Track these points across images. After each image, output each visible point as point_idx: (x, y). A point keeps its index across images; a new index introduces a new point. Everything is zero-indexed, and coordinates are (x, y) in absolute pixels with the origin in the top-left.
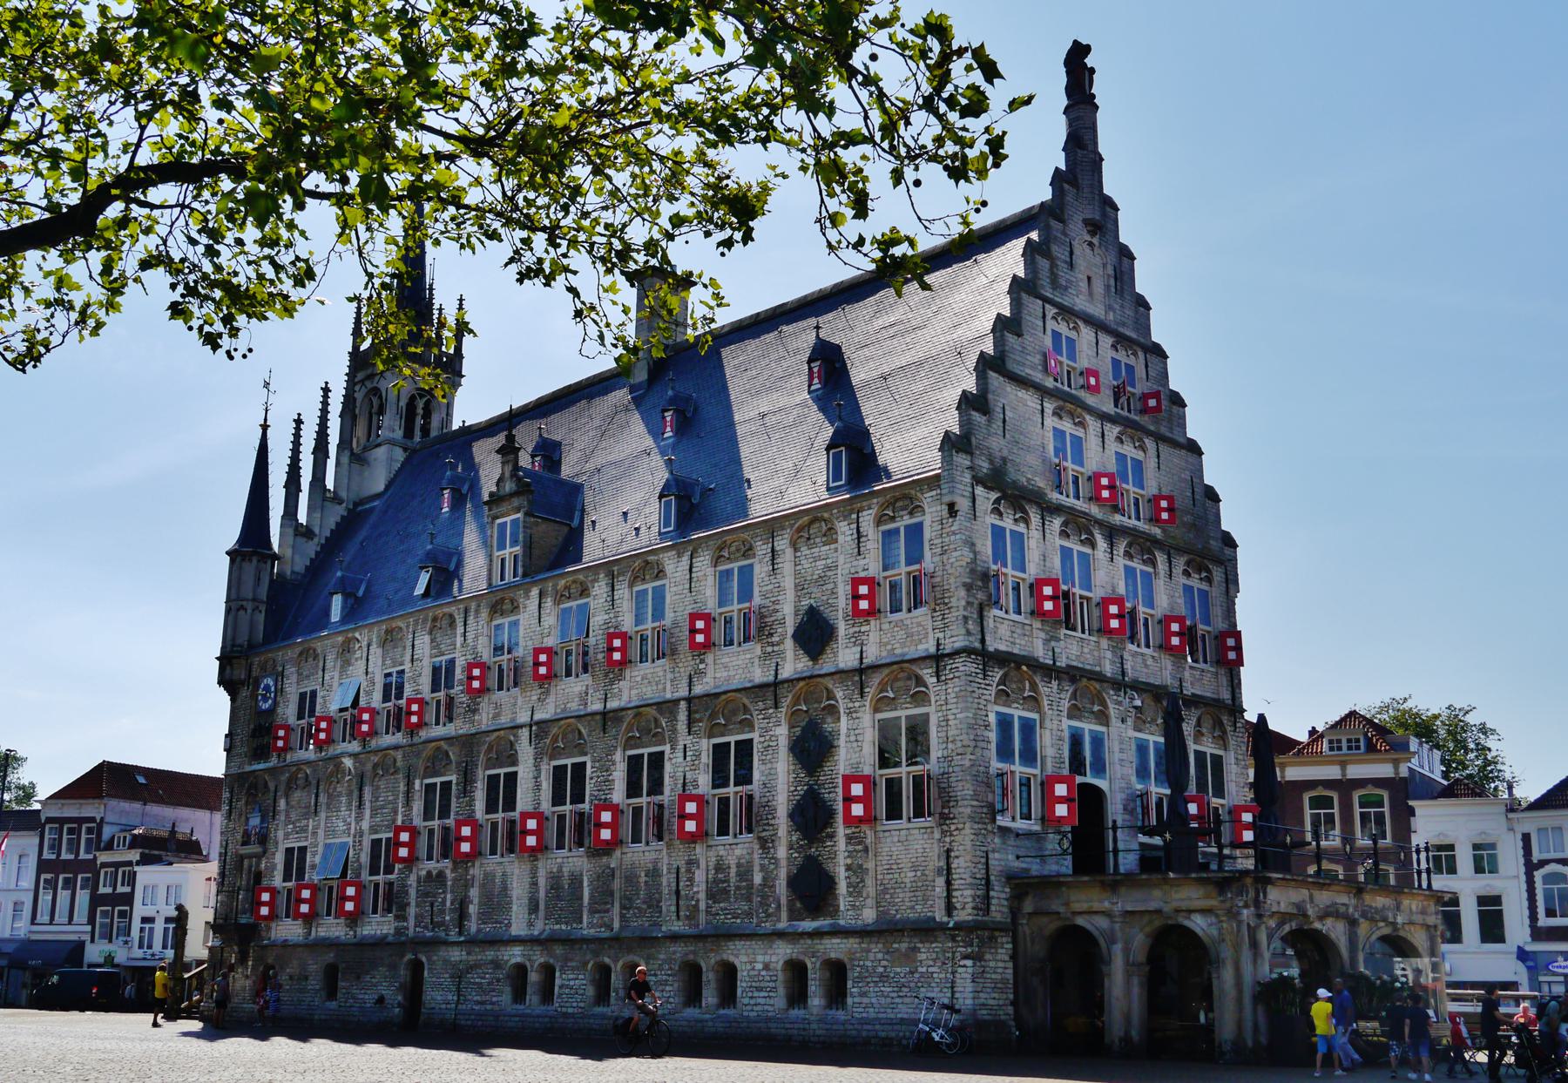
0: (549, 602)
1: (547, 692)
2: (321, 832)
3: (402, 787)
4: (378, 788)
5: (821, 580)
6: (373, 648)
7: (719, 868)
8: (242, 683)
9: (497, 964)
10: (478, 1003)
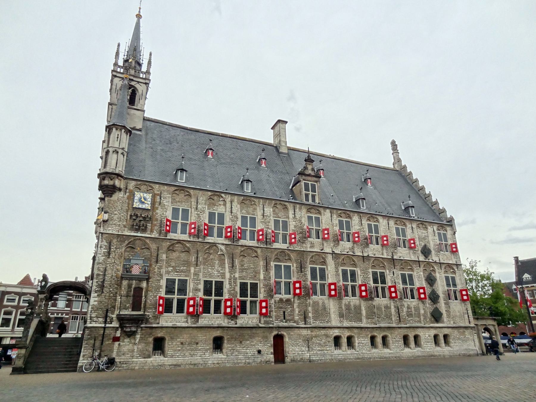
0: (335, 216)
1: (338, 244)
2: (201, 274)
3: (262, 263)
4: (242, 261)
5: (424, 238)
6: (235, 204)
7: (409, 307)
8: (120, 190)
9: (327, 336)
10: (319, 350)
